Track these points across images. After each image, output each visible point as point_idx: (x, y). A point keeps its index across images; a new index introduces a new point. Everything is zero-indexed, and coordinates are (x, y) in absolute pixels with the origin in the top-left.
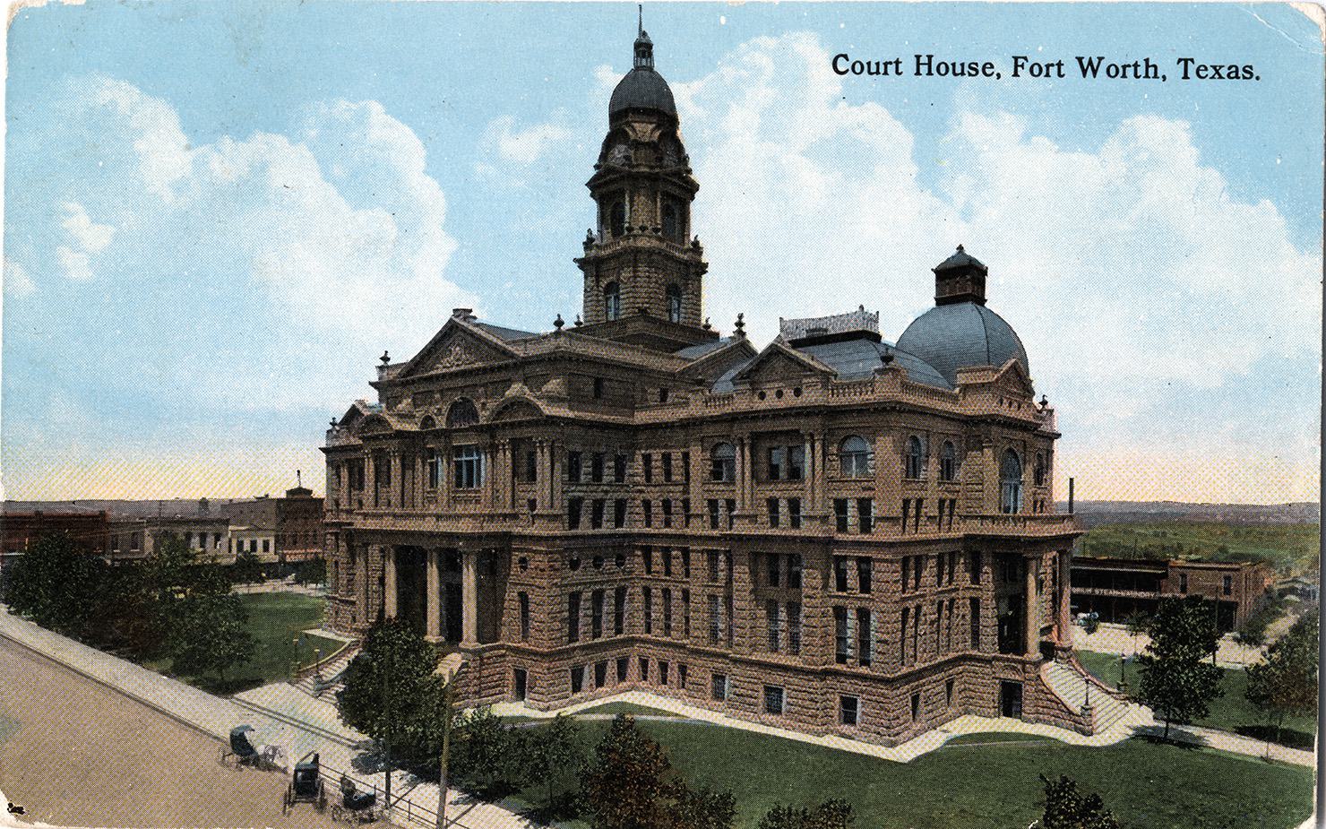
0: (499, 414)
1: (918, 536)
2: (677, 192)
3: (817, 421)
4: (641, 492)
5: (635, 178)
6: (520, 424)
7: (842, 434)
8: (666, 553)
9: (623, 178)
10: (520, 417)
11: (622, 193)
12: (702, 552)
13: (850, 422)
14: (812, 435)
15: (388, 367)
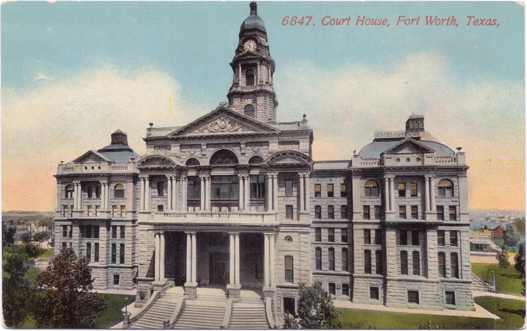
1: (301, 222)
8: (332, 230)
12: (359, 229)
15: (152, 128)
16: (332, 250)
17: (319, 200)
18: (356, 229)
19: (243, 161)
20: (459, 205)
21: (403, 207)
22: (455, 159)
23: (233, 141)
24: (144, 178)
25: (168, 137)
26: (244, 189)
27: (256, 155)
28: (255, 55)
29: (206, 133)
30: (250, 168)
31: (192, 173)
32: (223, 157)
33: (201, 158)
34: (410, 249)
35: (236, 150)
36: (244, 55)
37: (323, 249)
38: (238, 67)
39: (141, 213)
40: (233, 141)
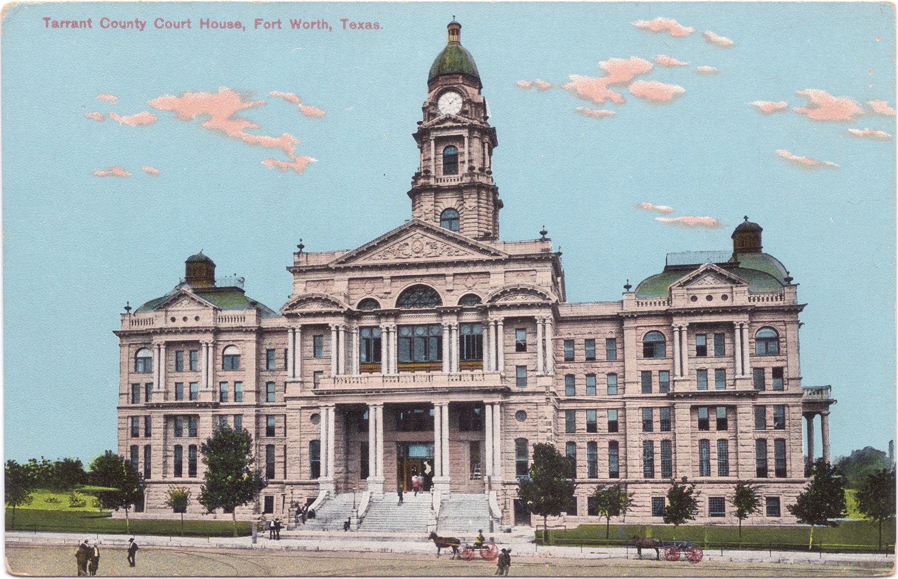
10: (520, 299)
16: (593, 445)
18: (630, 409)
19: (450, 301)
20: (787, 366)
21: (702, 372)
22: (781, 296)
23: (433, 271)
24: (294, 329)
25: (331, 266)
26: (451, 346)
27: (470, 292)
28: (459, 122)
29: (391, 260)
30: (459, 312)
31: (369, 321)
32: (419, 296)
33: (381, 298)
34: (714, 435)
35: (438, 286)
36: (442, 121)
37: (578, 444)
38: (428, 141)
39: (291, 382)
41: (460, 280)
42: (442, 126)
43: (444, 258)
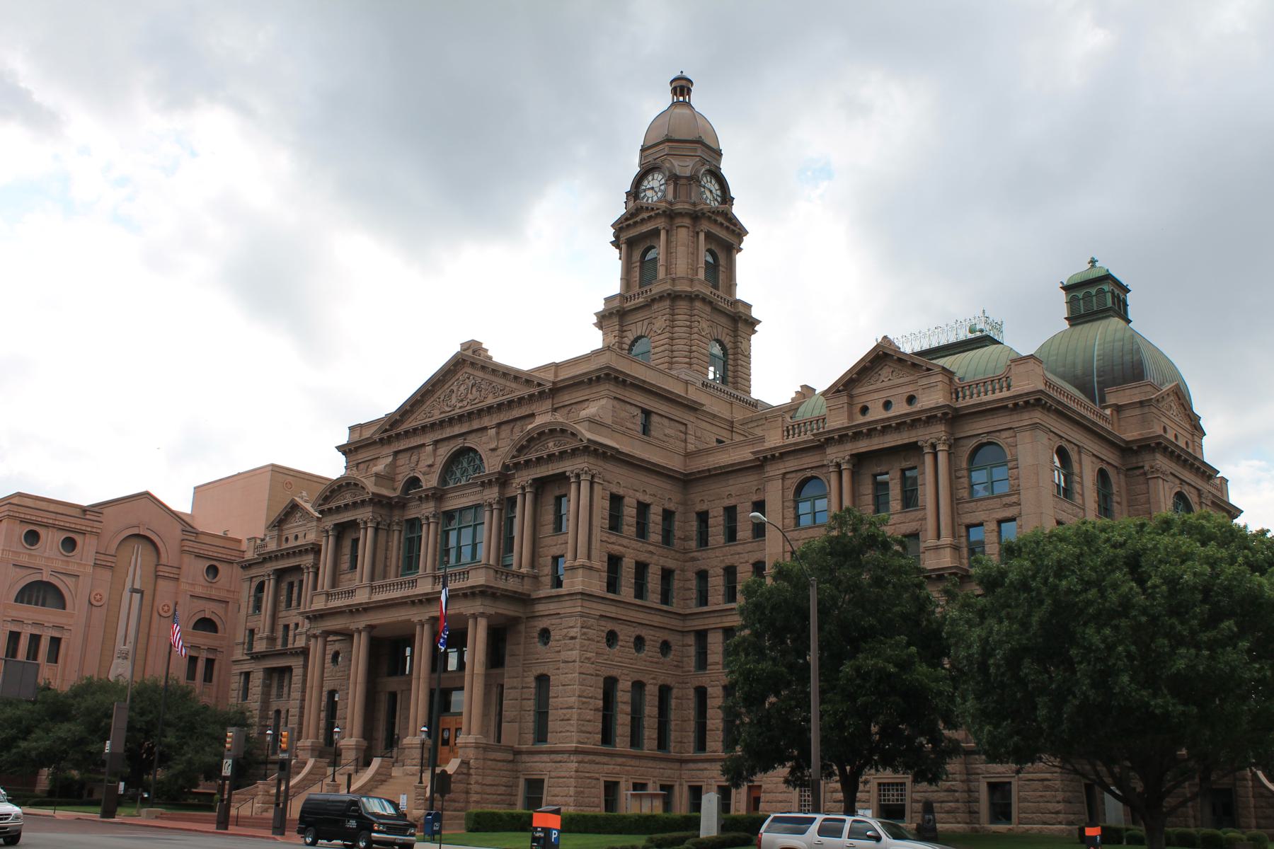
0: (521, 450)
2: (722, 234)
3: (938, 432)
4: (694, 559)
5: (671, 215)
6: (551, 457)
7: (973, 443)
9: (657, 215)
10: (552, 447)
11: (655, 233)
13: (980, 427)
14: (933, 446)
17: (704, 555)
23: (476, 425)
29: (437, 416)
40: (476, 425)
41: (505, 431)
42: (638, 219)
43: (491, 401)
